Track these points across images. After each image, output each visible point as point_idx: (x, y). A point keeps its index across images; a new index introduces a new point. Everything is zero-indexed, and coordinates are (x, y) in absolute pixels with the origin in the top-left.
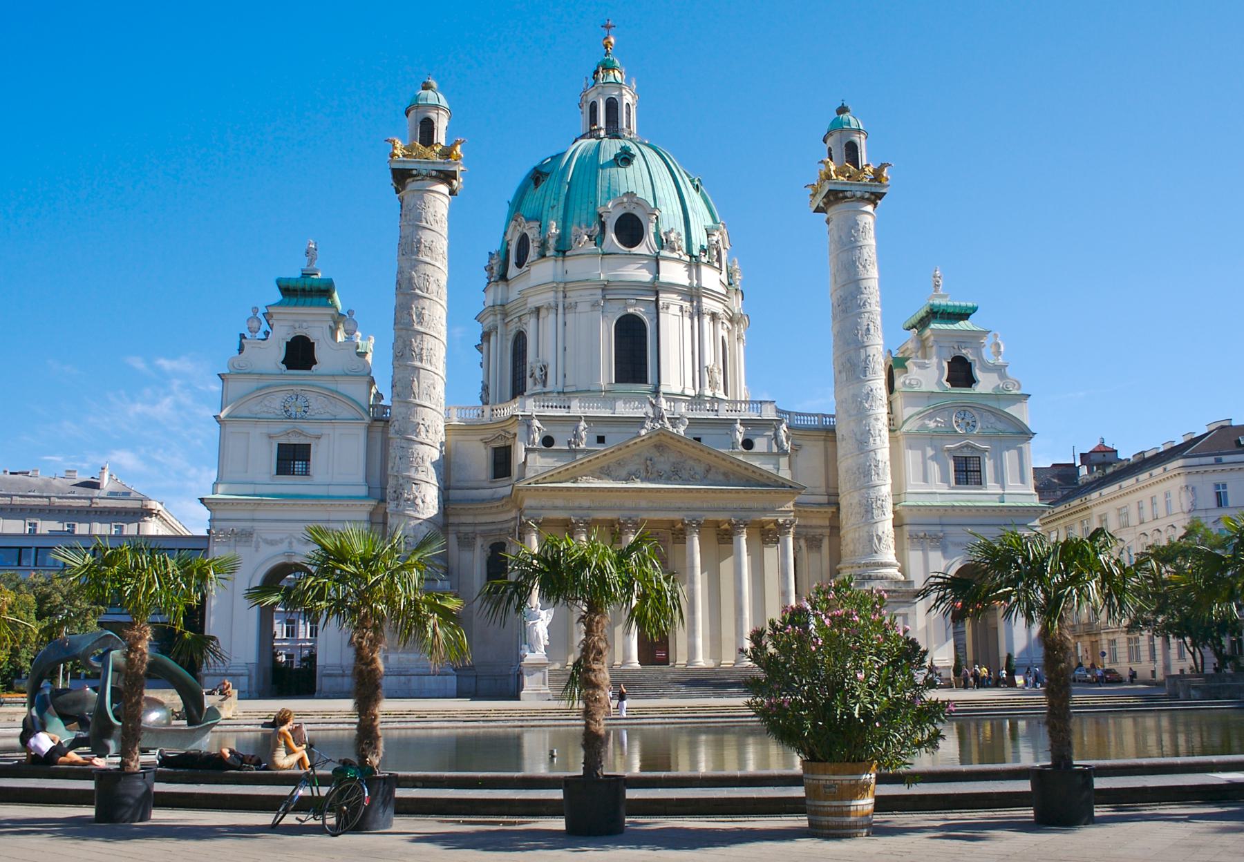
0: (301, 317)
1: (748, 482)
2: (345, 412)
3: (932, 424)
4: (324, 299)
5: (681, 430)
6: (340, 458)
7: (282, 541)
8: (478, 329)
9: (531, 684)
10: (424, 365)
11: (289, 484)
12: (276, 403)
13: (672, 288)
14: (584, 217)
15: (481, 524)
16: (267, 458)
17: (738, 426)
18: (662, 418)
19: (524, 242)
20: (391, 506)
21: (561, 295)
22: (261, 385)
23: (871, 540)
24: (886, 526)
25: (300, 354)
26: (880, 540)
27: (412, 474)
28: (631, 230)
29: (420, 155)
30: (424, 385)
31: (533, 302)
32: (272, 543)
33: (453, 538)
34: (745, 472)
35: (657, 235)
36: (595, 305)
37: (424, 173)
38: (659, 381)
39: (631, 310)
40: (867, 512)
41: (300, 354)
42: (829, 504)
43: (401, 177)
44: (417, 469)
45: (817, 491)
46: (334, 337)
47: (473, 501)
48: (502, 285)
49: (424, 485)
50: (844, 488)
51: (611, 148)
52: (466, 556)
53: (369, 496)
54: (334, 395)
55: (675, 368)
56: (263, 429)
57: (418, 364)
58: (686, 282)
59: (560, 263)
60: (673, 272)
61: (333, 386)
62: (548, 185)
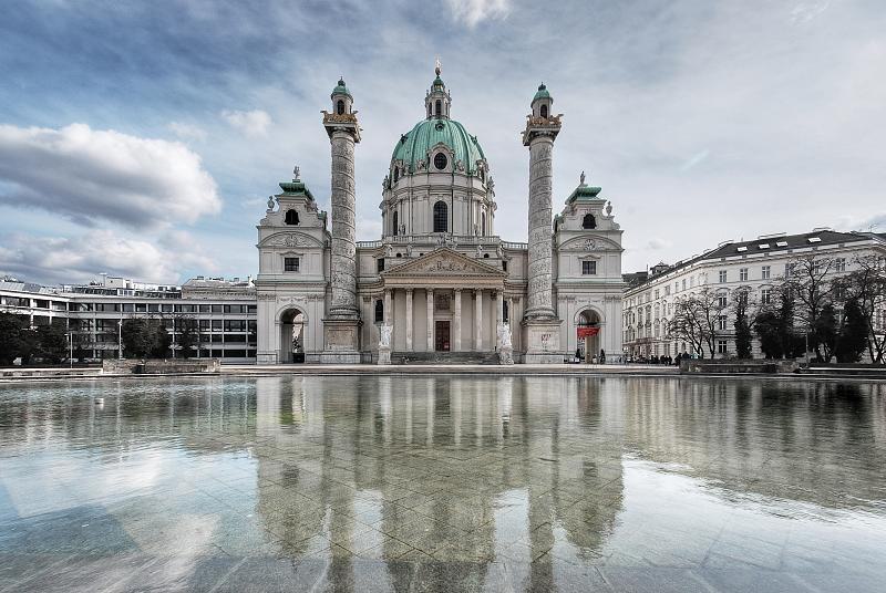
11: (291, 276)
13: (459, 188)
16: (280, 263)
24: (548, 293)
25: (292, 217)
28: (441, 161)
31: (399, 197)
41: (292, 217)
51: (435, 121)
52: (367, 306)
54: (308, 236)
62: (407, 143)
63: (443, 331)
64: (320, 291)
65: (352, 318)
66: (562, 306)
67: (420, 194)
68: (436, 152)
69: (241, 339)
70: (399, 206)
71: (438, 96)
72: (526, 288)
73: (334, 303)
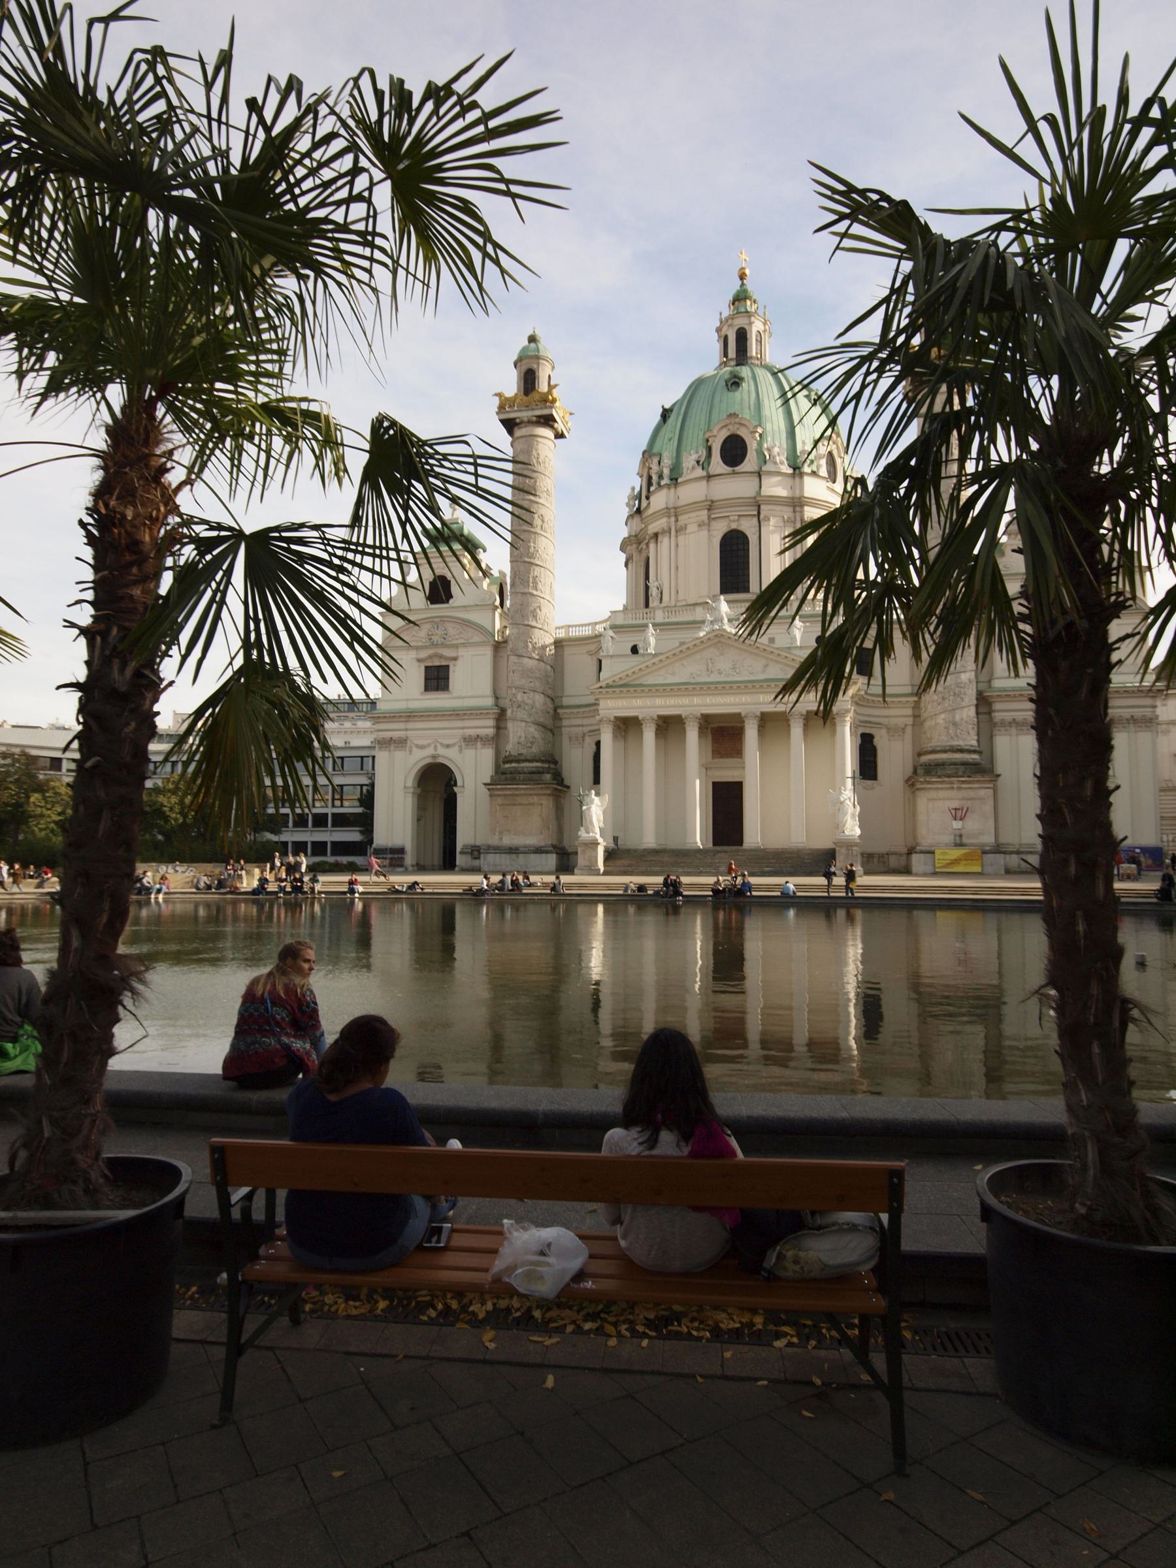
2: (477, 638)
6: (472, 679)
7: (429, 745)
8: (622, 557)
9: (581, 861)
11: (437, 700)
13: (775, 500)
14: (695, 445)
19: (650, 478)
20: (509, 712)
21: (673, 519)
25: (440, 591)
28: (734, 451)
31: (653, 528)
32: (422, 747)
37: (526, 419)
39: (734, 526)
40: (943, 699)
41: (440, 591)
43: (510, 425)
48: (637, 519)
59: (672, 490)
60: (774, 487)
62: (671, 419)
63: (727, 803)
64: (486, 727)
66: (1002, 743)
67: (691, 520)
68: (724, 434)
69: (341, 821)
70: (652, 546)
71: (740, 322)
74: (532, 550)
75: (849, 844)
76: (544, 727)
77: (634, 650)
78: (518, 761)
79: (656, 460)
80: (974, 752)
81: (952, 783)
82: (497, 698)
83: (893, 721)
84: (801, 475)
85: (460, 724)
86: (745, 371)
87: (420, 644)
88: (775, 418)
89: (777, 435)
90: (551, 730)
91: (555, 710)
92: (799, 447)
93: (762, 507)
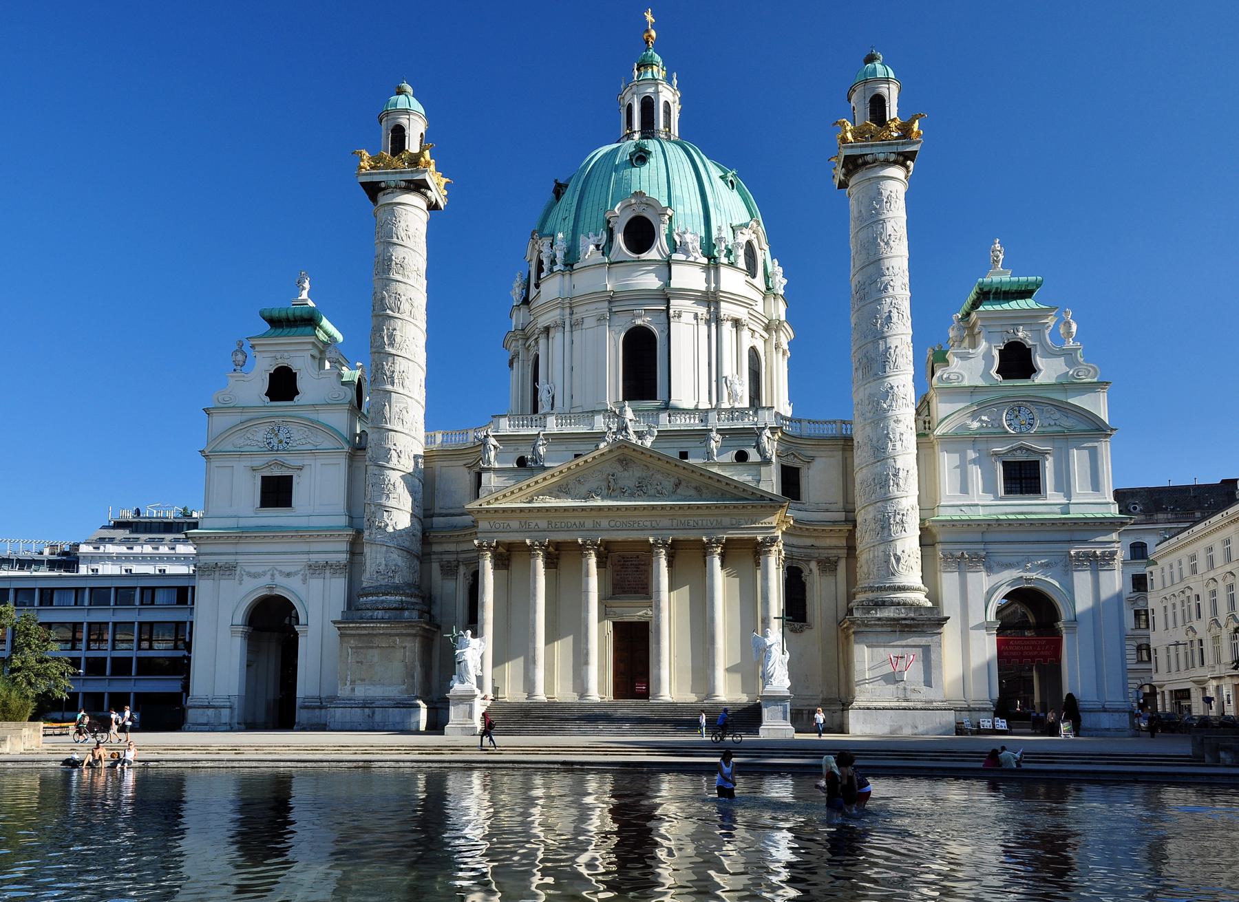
0: (283, 348)
1: (723, 496)
3: (975, 425)
4: (309, 329)
5: (648, 442)
6: (320, 490)
10: (397, 388)
12: (260, 435)
15: (464, 552)
17: (714, 434)
18: (626, 428)
22: (244, 418)
23: (887, 561)
25: (283, 385)
26: (898, 560)
27: (384, 501)
28: (641, 234)
29: (387, 166)
30: (395, 409)
33: (436, 567)
34: (717, 484)
35: (670, 237)
36: (601, 319)
38: (670, 397)
39: (639, 322)
40: (883, 528)
41: (283, 385)
42: (846, 521)
44: (388, 496)
45: (834, 507)
46: (321, 366)
47: (454, 528)
49: (395, 512)
50: (860, 502)
53: (351, 525)
55: (687, 383)
56: (247, 462)
57: (389, 387)
58: (703, 287)
59: (567, 277)
60: (689, 277)
61: (313, 416)
64: (338, 551)
65: (406, 613)
68: (629, 215)
72: (851, 535)
73: (367, 580)
74: (398, 339)
75: (776, 700)
76: (408, 551)
77: (522, 462)
78: (376, 594)
79: (547, 241)
80: (918, 589)
81: (891, 626)
82: (351, 517)
83: (824, 554)
84: (717, 268)
85: (305, 548)
86: (652, 145)
87: (255, 449)
88: (686, 200)
89: (689, 219)
90: (418, 557)
91: (424, 534)
92: (715, 234)
93: (672, 302)
